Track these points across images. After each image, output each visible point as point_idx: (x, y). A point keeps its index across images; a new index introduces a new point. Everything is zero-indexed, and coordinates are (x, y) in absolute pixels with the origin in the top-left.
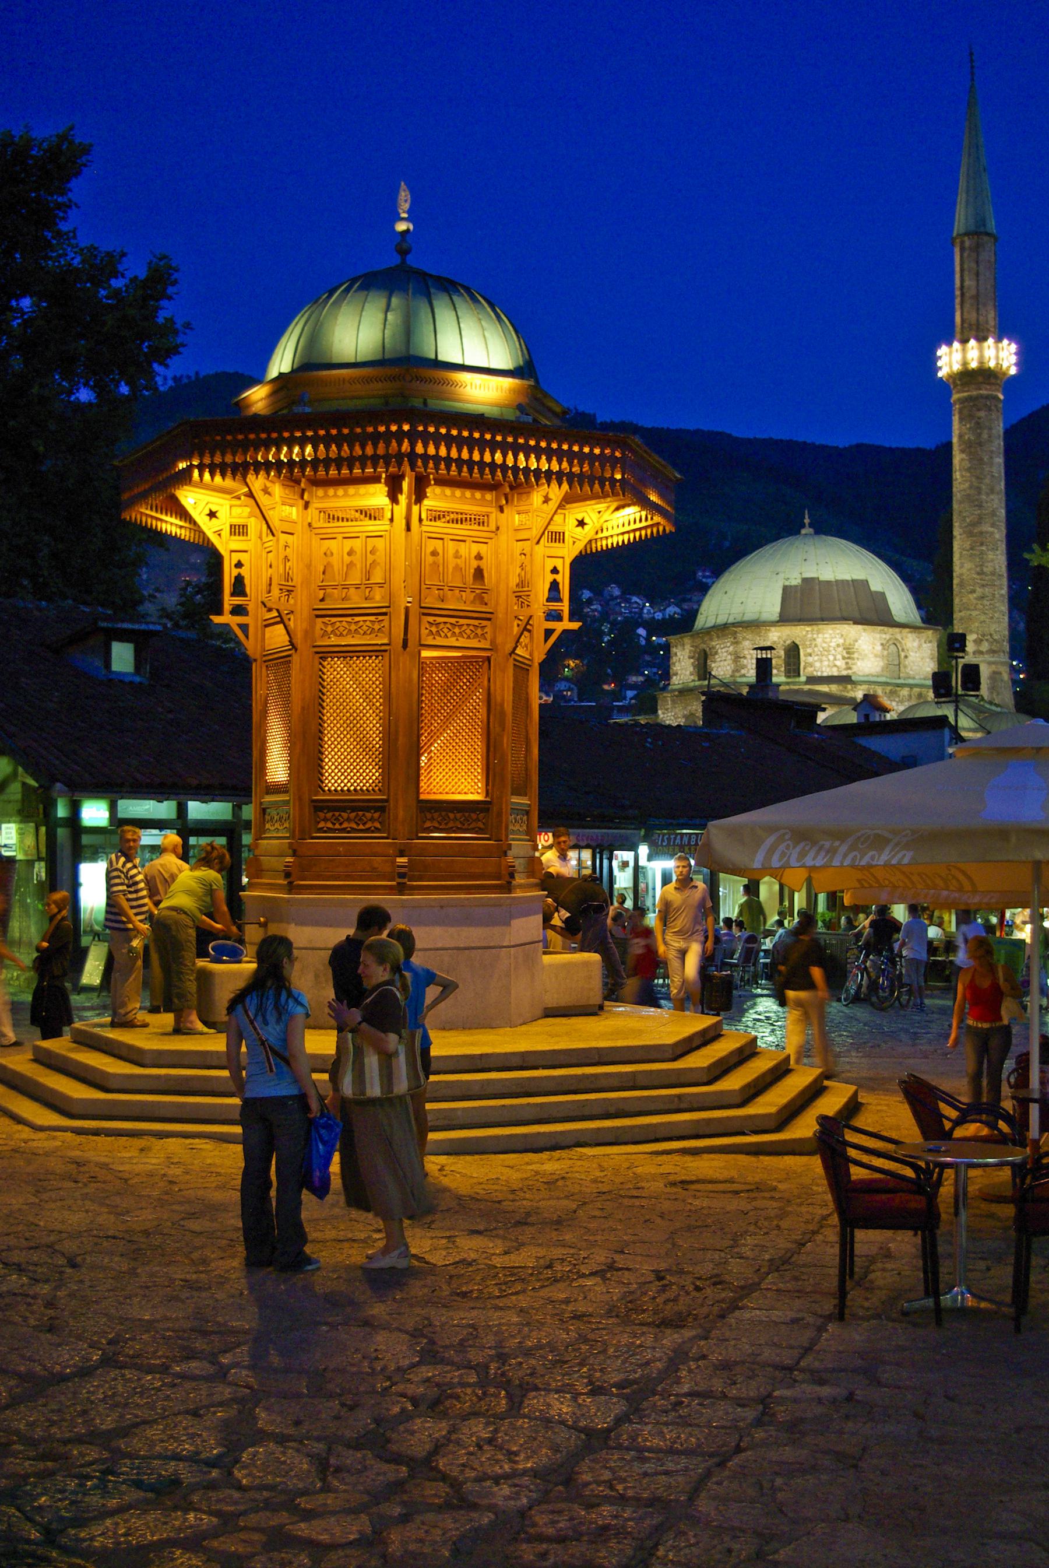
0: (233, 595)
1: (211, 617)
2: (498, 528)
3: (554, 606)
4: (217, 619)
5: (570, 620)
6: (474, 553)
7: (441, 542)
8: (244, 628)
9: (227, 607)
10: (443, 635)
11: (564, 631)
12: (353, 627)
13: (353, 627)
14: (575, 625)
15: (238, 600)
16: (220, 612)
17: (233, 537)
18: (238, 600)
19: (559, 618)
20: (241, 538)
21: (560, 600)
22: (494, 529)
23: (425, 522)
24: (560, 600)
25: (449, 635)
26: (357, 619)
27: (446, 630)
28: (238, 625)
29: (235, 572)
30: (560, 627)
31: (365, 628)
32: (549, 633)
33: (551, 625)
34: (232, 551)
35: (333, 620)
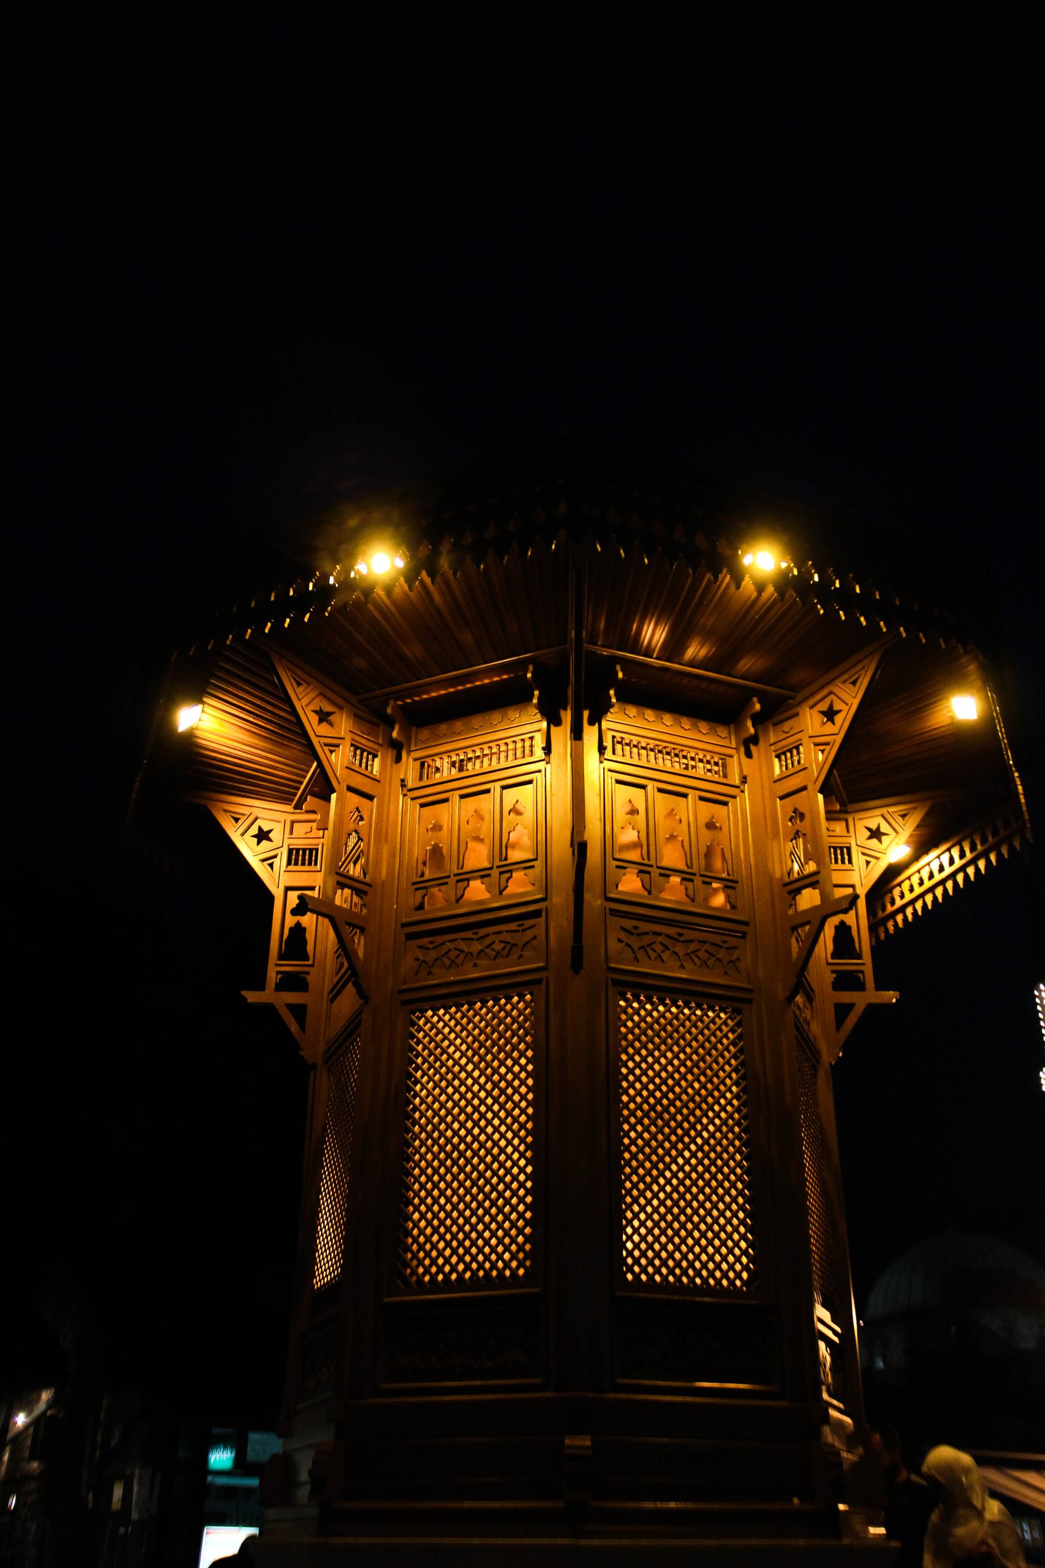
0: (281, 957)
1: (243, 993)
2: (744, 780)
3: (847, 964)
4: (252, 997)
5: (881, 985)
6: (703, 819)
7: (641, 791)
8: (299, 1012)
9: (272, 975)
10: (653, 955)
11: (872, 1009)
12: (476, 947)
13: (476, 947)
14: (892, 997)
15: (290, 966)
16: (261, 986)
17: (292, 868)
18: (290, 966)
19: (861, 987)
20: (306, 868)
21: (859, 956)
22: (737, 782)
23: (608, 754)
24: (859, 956)
25: (665, 956)
26: (482, 932)
27: (659, 948)
28: (291, 1007)
29: (291, 921)
30: (860, 1000)
31: (498, 947)
32: (842, 1011)
33: (847, 997)
34: (288, 889)
35: (438, 939)
